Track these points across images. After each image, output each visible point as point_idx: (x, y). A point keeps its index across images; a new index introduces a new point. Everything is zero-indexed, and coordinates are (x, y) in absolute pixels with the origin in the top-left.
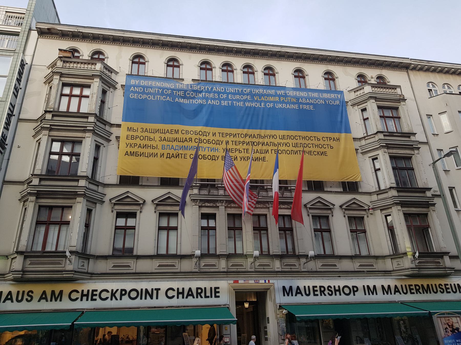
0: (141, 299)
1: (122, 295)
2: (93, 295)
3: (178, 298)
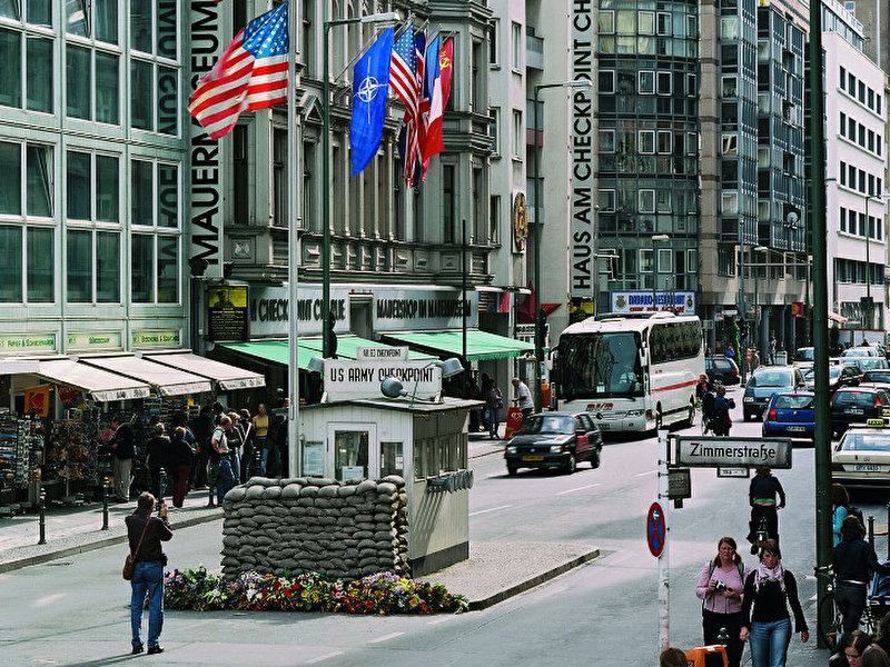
0: (589, 70)
1: (583, 101)
2: (582, 144)
3: (589, 11)
